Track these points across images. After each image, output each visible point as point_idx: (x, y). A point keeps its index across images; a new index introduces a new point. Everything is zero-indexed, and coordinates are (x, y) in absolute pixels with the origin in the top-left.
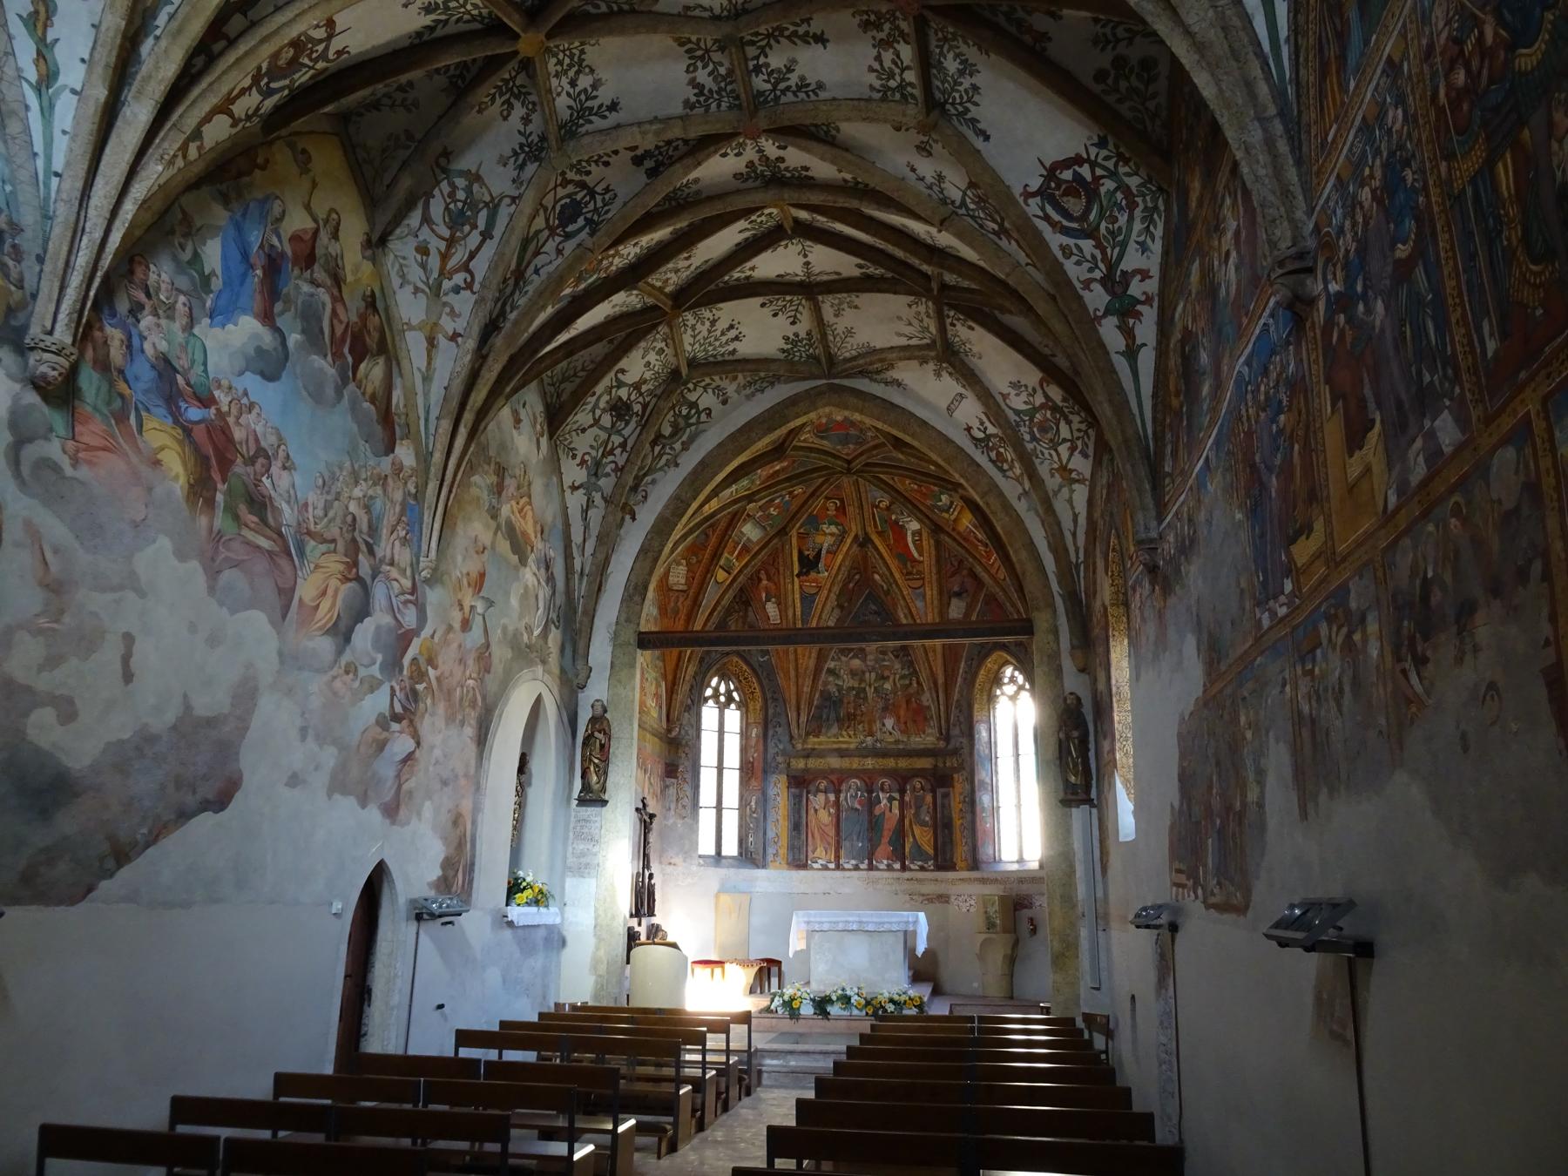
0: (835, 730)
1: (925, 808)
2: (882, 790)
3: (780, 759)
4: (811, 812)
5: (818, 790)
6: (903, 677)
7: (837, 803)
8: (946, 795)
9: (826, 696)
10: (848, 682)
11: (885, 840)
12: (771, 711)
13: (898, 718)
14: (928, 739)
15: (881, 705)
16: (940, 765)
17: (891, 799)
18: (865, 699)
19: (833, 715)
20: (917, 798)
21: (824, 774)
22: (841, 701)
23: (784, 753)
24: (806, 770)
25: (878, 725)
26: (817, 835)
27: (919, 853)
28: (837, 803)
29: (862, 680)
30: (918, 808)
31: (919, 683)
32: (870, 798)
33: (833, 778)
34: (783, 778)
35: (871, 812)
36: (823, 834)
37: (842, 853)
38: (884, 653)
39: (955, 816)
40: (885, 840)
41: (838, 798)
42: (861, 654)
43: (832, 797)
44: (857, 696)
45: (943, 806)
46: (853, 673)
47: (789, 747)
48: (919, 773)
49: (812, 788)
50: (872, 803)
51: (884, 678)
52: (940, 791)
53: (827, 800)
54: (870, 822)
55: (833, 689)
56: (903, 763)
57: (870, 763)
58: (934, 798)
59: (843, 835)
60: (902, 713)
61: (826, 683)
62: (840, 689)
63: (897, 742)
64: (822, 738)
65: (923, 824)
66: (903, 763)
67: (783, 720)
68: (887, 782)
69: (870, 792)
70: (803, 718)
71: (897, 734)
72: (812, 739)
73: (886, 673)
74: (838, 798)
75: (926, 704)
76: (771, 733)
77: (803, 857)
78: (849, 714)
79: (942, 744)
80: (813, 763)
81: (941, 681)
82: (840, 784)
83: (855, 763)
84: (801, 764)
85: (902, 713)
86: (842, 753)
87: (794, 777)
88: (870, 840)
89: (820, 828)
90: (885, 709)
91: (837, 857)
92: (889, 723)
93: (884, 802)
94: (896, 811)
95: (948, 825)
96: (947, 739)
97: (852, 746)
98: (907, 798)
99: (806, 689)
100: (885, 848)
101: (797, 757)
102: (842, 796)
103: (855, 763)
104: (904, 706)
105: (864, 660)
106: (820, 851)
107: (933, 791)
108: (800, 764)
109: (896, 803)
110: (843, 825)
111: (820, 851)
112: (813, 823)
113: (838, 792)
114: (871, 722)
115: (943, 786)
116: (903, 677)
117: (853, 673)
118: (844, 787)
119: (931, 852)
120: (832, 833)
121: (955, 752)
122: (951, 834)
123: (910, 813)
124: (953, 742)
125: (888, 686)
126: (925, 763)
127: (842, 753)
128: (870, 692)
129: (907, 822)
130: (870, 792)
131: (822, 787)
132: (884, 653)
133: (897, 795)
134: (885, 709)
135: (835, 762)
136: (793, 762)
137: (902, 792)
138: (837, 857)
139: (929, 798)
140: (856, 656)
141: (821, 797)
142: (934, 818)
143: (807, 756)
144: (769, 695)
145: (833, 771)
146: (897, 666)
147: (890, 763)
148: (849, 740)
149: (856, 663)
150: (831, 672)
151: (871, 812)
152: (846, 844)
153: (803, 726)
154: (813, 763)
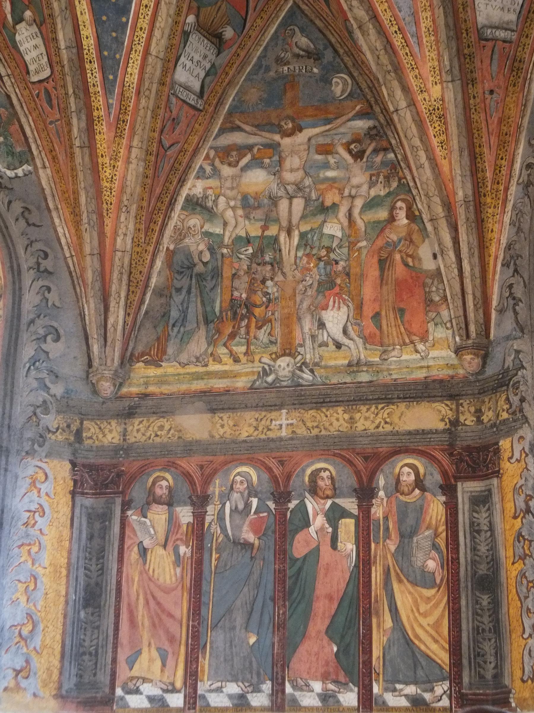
0: (198, 344)
1: (424, 537)
2: (314, 490)
3: (51, 420)
4: (133, 555)
5: (152, 499)
6: (371, 204)
7: (198, 532)
8: (482, 500)
9: (182, 266)
10: (236, 225)
11: (319, 624)
12: (30, 300)
13: (359, 307)
14: (436, 354)
15: (315, 275)
16: (468, 419)
17: (335, 515)
18: (277, 264)
19: (195, 308)
20: (403, 511)
21: (167, 456)
22: (217, 273)
23: (65, 405)
24: (125, 449)
25: (308, 324)
26: (141, 611)
27: (411, 662)
28: (198, 532)
29: (268, 220)
30: (407, 536)
31: (411, 216)
32: (281, 514)
33: (190, 465)
34: (60, 471)
35: (282, 552)
36: (160, 616)
37: (205, 663)
38: (326, 150)
39: (506, 554)
40: (319, 624)
41: (199, 517)
42: (270, 157)
43: (185, 515)
44: (261, 251)
45: (475, 529)
46: (248, 204)
47: (83, 392)
48: (411, 443)
49: (137, 493)
50: (285, 526)
51: (326, 210)
52: (466, 489)
53: (173, 522)
54: (281, 577)
55: (196, 245)
56: (367, 420)
57: (283, 423)
58: (452, 508)
59: (209, 613)
60: (368, 292)
61: (181, 234)
62: (214, 244)
63: (355, 366)
64: (169, 368)
65: (424, 580)
66: (367, 420)
67: (67, 323)
68: (326, 468)
69: (282, 496)
70: (118, 316)
71: (356, 348)
72: (142, 371)
73: (330, 198)
74: (199, 517)
75: (428, 264)
76: (27, 351)
77: (104, 678)
78: (234, 304)
79: (471, 362)
80: (142, 431)
81: (461, 192)
82: (207, 480)
83: (246, 426)
84: (111, 434)
85: (368, 292)
86: (216, 402)
87: (91, 468)
88: (280, 626)
89: (151, 598)
90: (327, 285)
91: (192, 676)
92: (335, 318)
93: (319, 522)
94: (348, 545)
95: (488, 582)
96: (484, 349)
97: (241, 383)
98: (378, 511)
99: (124, 242)
100: (317, 648)
101: (100, 416)
102: (211, 510)
103: (246, 426)
104: (374, 272)
105: (277, 170)
106: (148, 663)
107: (448, 489)
108: (108, 434)
109: (348, 526)
110: (210, 587)
111: (148, 663)
112: (133, 589)
113: (200, 502)
114: (290, 321)
115: (474, 475)
116: (371, 204)
117: (248, 204)
118: (216, 488)
119: (442, 656)
120: (180, 607)
121: (504, 381)
122: (496, 605)
123: (386, 549)
124: (497, 353)
125: (333, 229)
126: (427, 417)
127: (216, 402)
128: (289, 246)
129: (377, 575)
130: (282, 496)
131: (161, 490)
132: (326, 150)
133: (350, 504)
134: (327, 285)
135: (195, 425)
136: (91, 429)
137: (365, 493)
138: (192, 676)
139: (436, 509)
140: (257, 163)
141: (158, 516)
142: (451, 563)
143: (130, 413)
144: (26, 261)
145: (190, 448)
146: (359, 177)
147: (336, 420)
148: (233, 367)
149: (257, 179)
150: (195, 205)
151: (282, 552)
152: (216, 639)
153: (116, 334)
154: (142, 431)
